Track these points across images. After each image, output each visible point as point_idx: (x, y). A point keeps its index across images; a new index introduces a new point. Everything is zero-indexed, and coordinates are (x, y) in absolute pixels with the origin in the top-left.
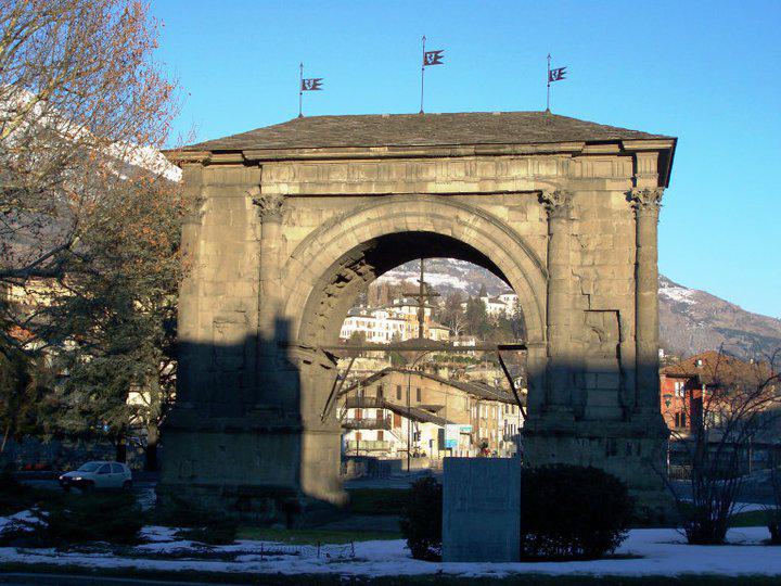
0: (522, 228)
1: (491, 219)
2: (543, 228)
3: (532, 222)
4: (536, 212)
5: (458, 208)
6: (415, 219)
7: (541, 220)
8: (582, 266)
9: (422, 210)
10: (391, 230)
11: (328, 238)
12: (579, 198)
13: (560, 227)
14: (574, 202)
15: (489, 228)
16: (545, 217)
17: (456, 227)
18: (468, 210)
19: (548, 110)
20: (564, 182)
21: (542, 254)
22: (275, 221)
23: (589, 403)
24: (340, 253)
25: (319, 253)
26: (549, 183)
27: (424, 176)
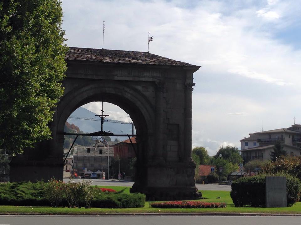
1: (136, 90)
3: (149, 93)
7: (153, 91)
26: (158, 79)
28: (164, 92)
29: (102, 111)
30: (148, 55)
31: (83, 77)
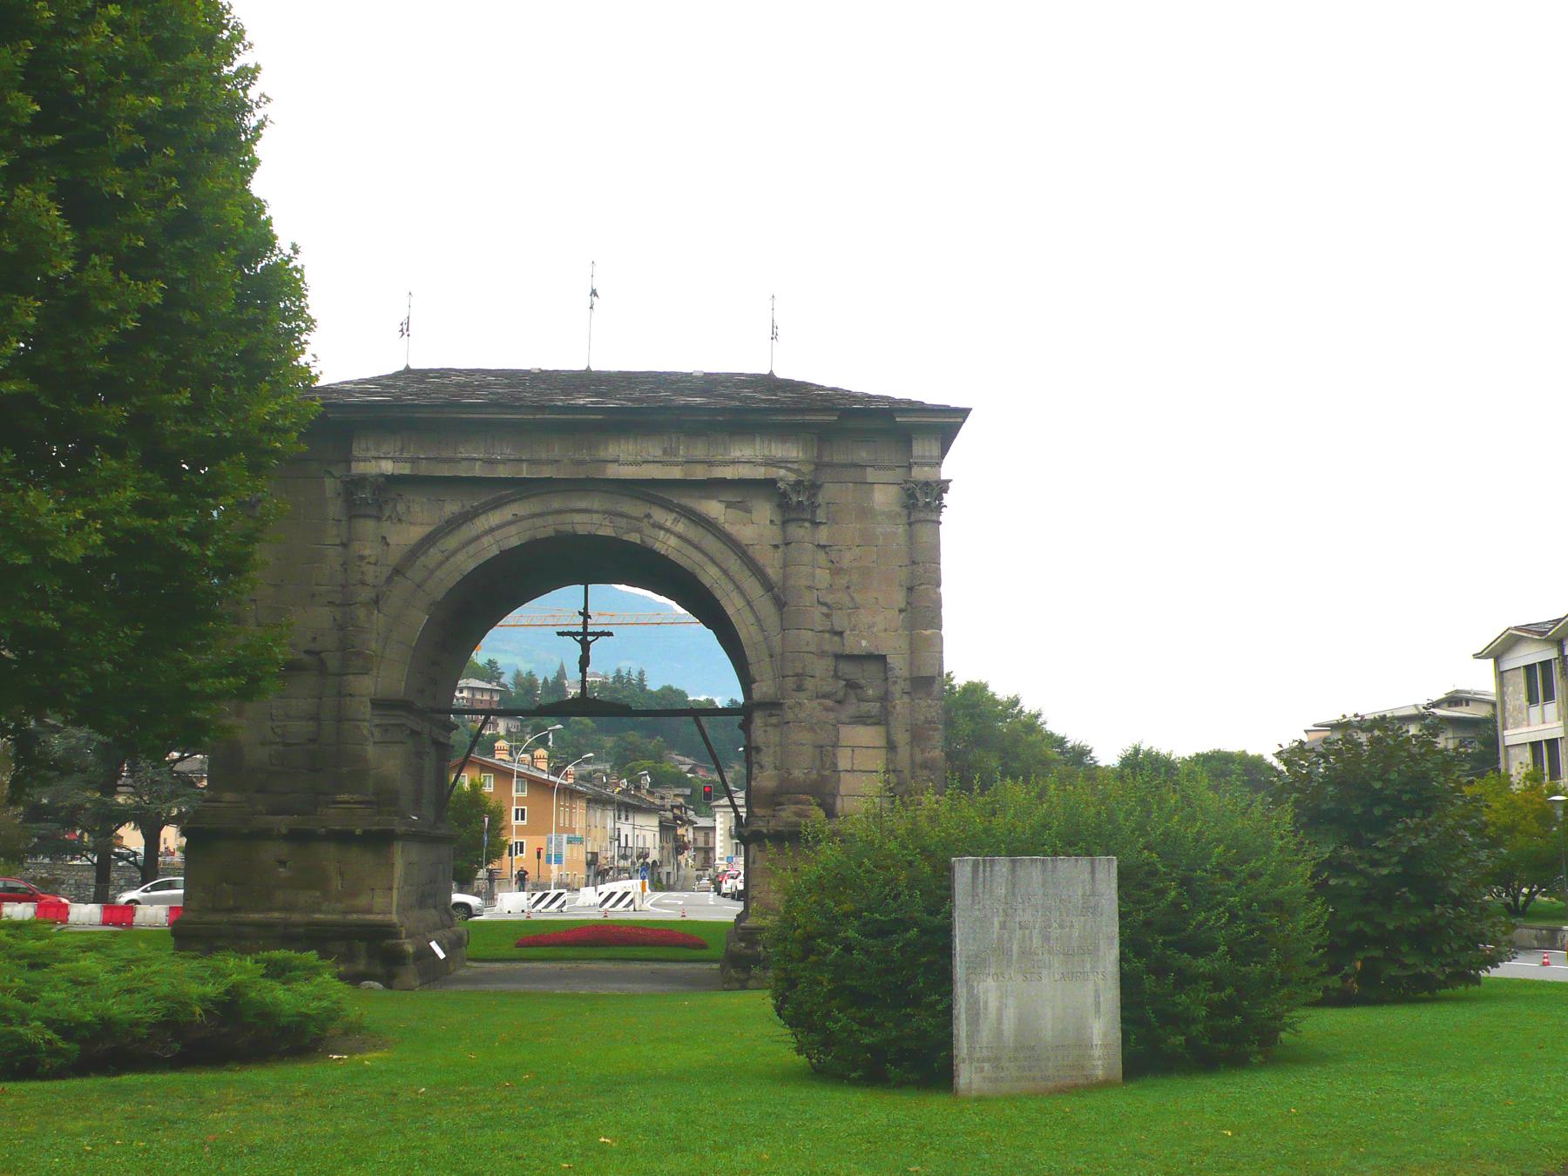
2: (772, 533)
4: (764, 511)
5: (648, 501)
7: (771, 521)
8: (831, 588)
10: (550, 532)
11: (451, 542)
12: (829, 492)
13: (798, 532)
14: (821, 498)
15: (694, 533)
16: (778, 520)
17: (648, 531)
18: (667, 506)
19: (771, 371)
21: (773, 572)
22: (370, 516)
24: (472, 565)
25: (441, 564)
26: (789, 470)
27: (602, 454)
28: (816, 524)
29: (585, 615)
30: (768, 382)
31: (478, 471)
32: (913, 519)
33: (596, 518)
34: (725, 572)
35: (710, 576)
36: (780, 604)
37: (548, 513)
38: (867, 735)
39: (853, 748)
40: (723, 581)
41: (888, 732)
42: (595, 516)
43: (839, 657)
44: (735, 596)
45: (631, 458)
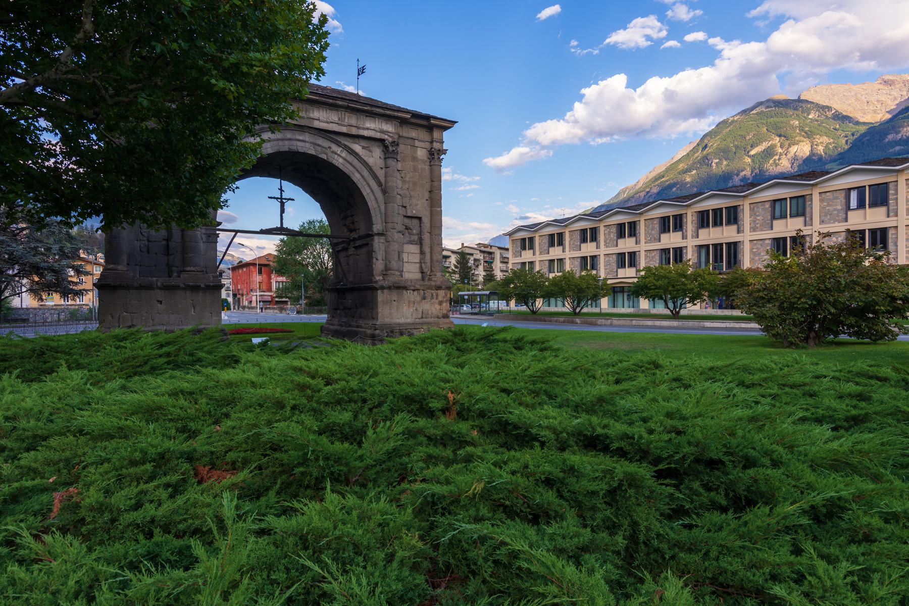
0: (370, 161)
2: (381, 163)
3: (375, 157)
6: (302, 144)
9: (307, 139)
12: (401, 148)
13: (391, 162)
15: (350, 158)
16: (382, 157)
17: (330, 154)
18: (338, 144)
20: (396, 137)
23: (405, 270)
26: (389, 136)
27: (312, 115)
32: (432, 163)
33: (307, 145)
34: (362, 176)
35: (356, 177)
36: (384, 192)
37: (286, 140)
38: (415, 249)
39: (408, 253)
40: (362, 180)
41: (421, 248)
42: (307, 144)
43: (405, 216)
44: (366, 187)
45: (325, 120)
